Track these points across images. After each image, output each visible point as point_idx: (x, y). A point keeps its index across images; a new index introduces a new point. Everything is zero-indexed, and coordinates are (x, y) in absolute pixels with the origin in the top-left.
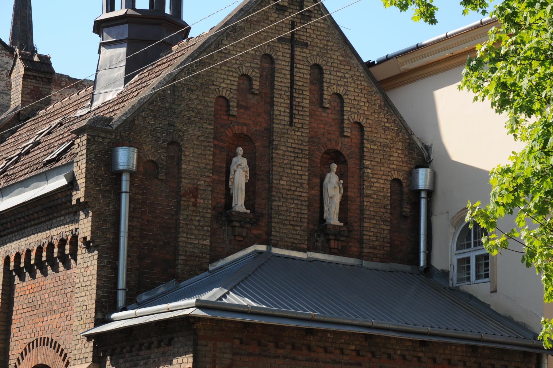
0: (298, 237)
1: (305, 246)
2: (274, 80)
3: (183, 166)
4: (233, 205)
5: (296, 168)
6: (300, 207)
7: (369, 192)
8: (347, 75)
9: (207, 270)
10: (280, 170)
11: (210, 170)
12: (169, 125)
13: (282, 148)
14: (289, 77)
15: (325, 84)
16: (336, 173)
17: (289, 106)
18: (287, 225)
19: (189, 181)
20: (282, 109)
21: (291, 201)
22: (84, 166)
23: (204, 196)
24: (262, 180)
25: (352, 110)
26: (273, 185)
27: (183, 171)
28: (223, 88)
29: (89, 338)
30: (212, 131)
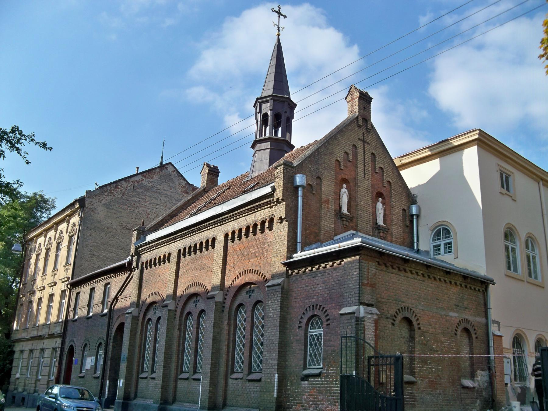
0: (369, 229)
1: (371, 234)
2: (357, 157)
3: (323, 189)
4: (342, 211)
5: (367, 197)
6: (369, 215)
7: (394, 213)
8: (384, 160)
9: (333, 239)
10: (361, 197)
11: (333, 192)
12: (317, 169)
13: (361, 187)
14: (363, 156)
15: (376, 162)
16: (381, 203)
17: (363, 169)
18: (364, 223)
19: (325, 196)
20: (361, 170)
21: (365, 212)
22: (282, 182)
23: (331, 204)
24: (354, 201)
25: (387, 175)
26: (359, 204)
27: (322, 191)
28: (338, 156)
29: (285, 264)
30: (334, 175)
